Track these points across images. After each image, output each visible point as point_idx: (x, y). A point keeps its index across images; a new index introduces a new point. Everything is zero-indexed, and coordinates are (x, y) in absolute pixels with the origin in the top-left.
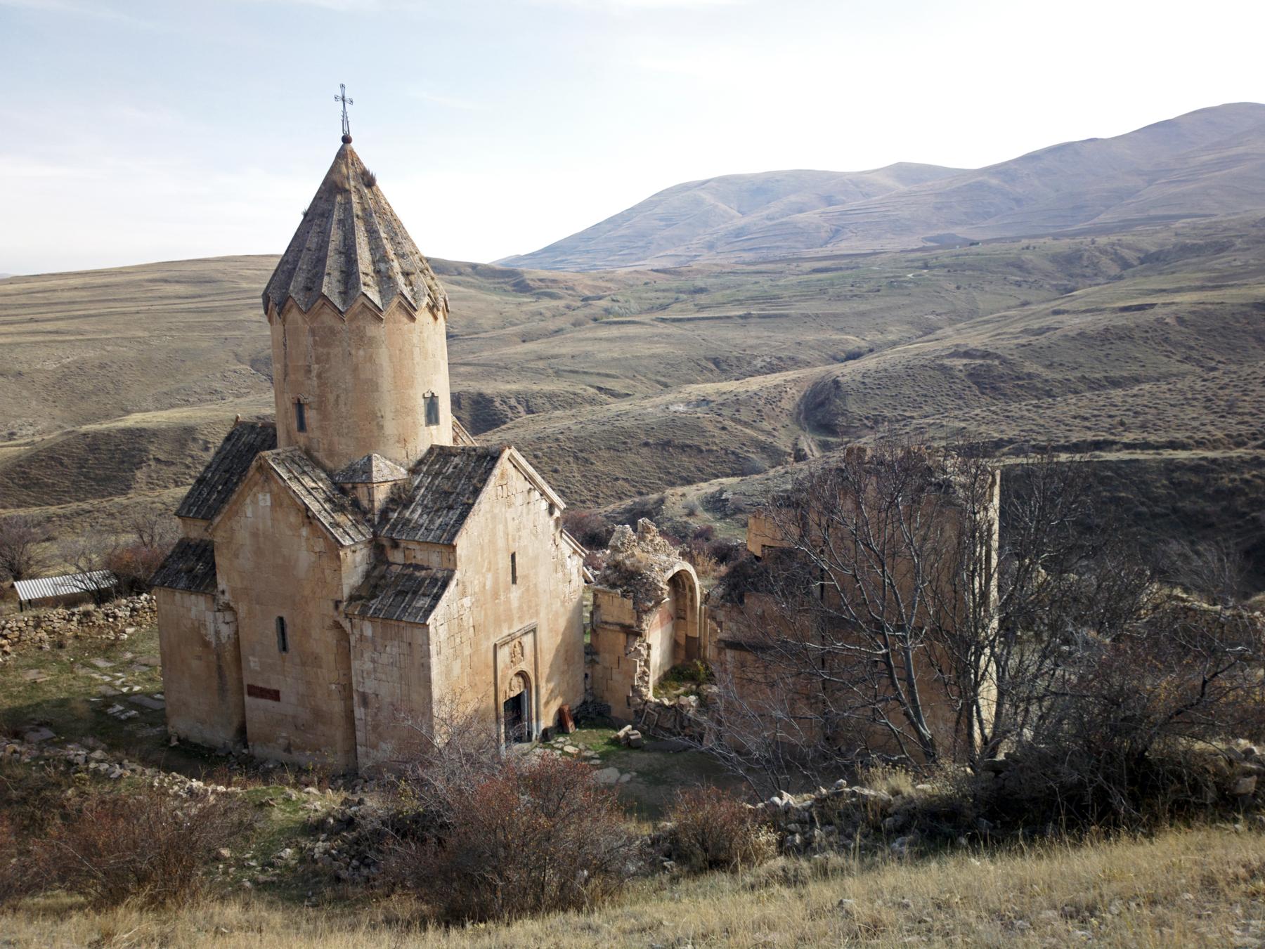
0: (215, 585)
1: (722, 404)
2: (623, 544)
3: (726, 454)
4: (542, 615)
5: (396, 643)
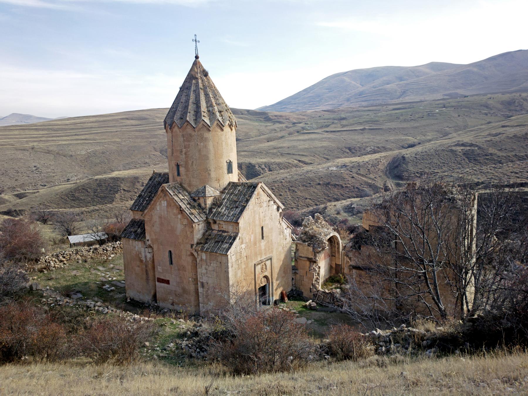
0: (145, 237)
1: (352, 167)
2: (308, 224)
3: (354, 188)
4: (274, 252)
5: (215, 262)
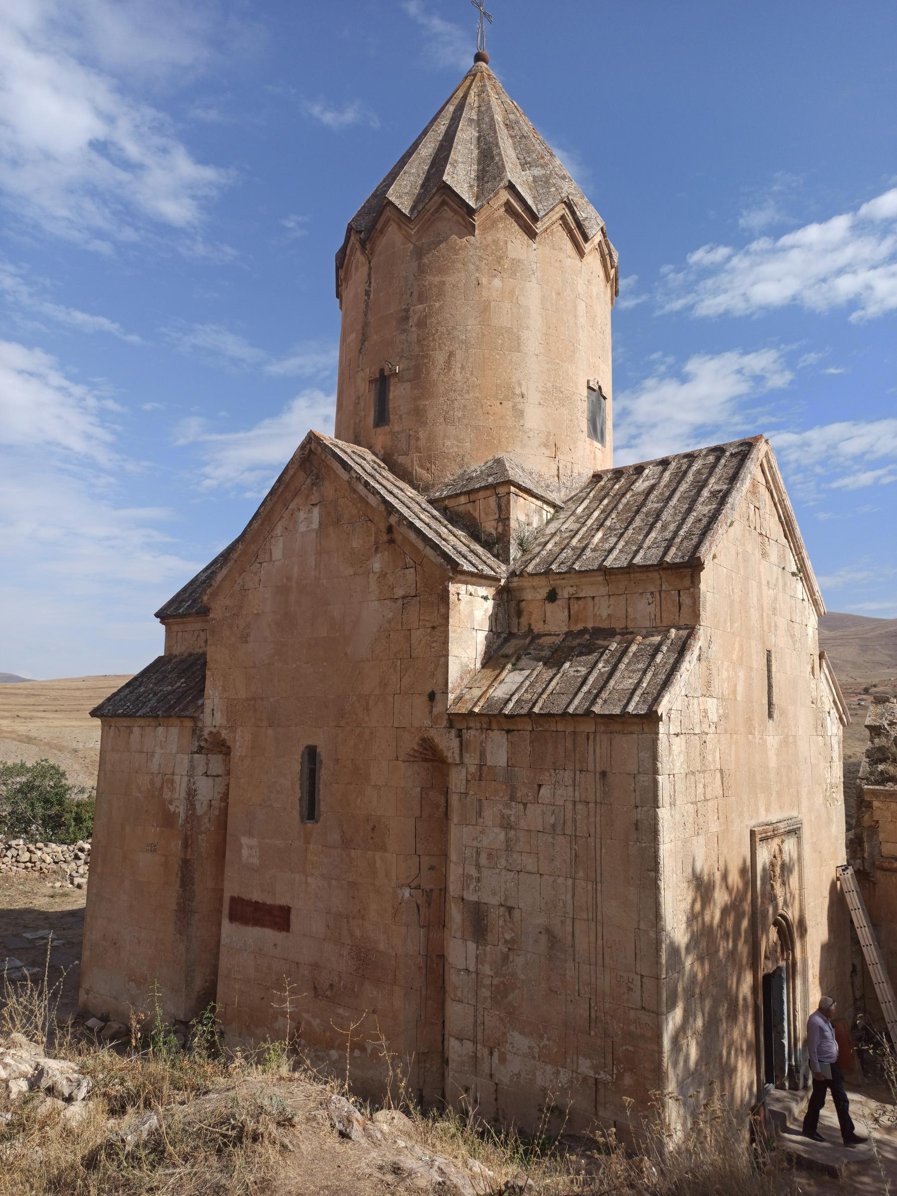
4: (805, 803)
5: (567, 775)
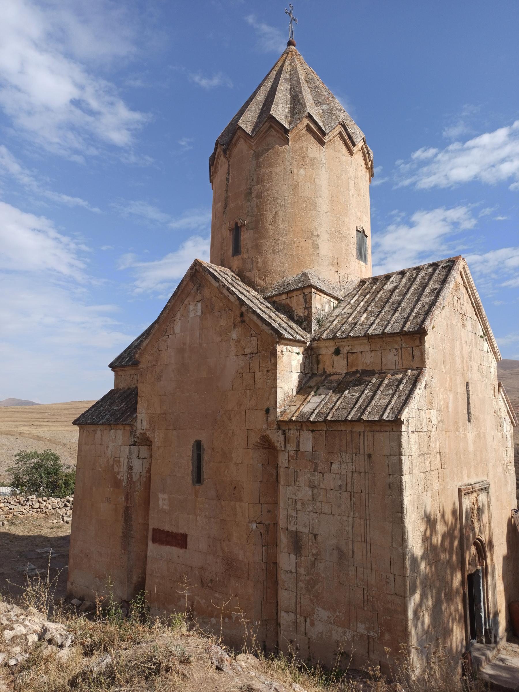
5: (348, 457)
